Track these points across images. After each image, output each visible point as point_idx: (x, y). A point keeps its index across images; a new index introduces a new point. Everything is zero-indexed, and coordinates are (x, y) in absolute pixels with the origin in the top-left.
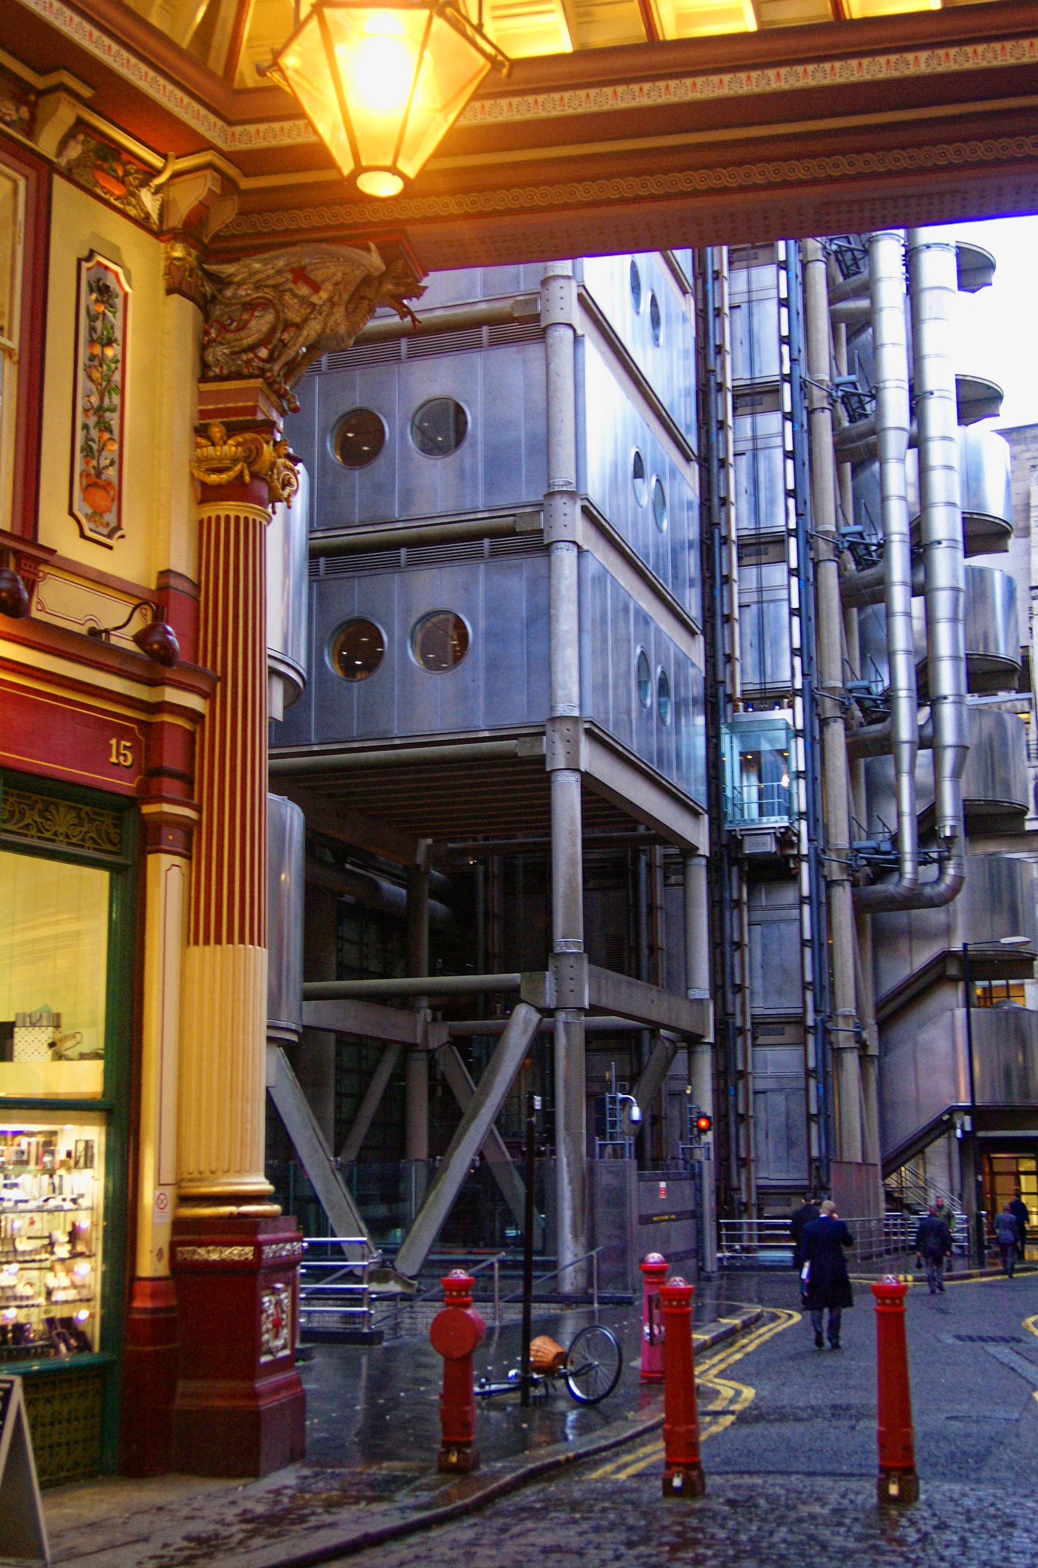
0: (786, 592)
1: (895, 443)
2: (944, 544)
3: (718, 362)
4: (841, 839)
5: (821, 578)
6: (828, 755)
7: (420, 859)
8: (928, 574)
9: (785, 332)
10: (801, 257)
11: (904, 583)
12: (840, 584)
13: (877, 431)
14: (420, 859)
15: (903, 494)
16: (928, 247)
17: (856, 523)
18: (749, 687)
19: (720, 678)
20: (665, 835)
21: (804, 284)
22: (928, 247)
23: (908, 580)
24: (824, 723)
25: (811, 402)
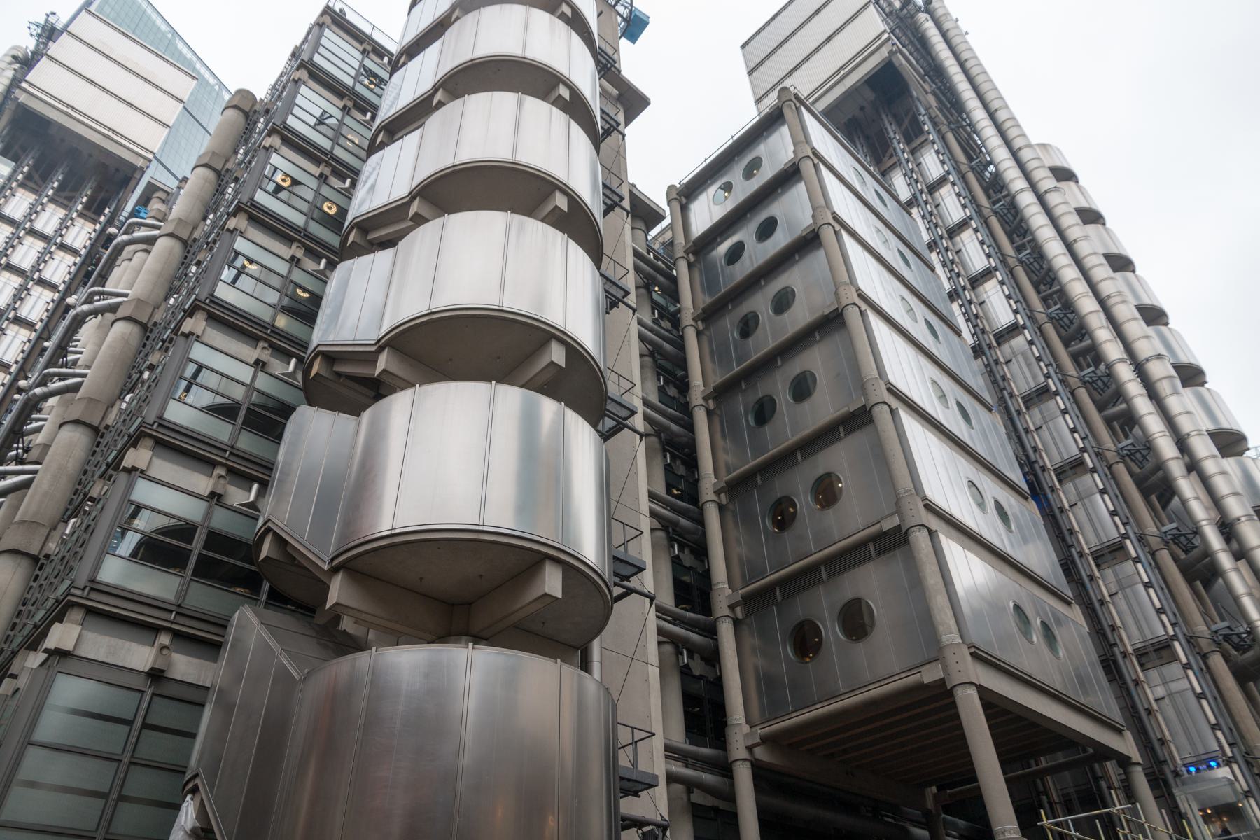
0: (1137, 576)
1: (1176, 469)
2: (1243, 519)
3: (1038, 456)
4: (1201, 628)
5: (1160, 562)
6: (1219, 681)
7: (930, 804)
8: (1240, 542)
9: (1072, 426)
10: (1105, 463)
11: (1224, 550)
12: (1178, 566)
13: (1160, 466)
14: (930, 804)
15: (1195, 495)
16: (1147, 360)
17: (1171, 523)
18: (1138, 646)
19: (1112, 641)
20: (1105, 753)
21: (1114, 477)
22: (1147, 360)
23: (1224, 546)
24: (1204, 657)
25: (1107, 461)
